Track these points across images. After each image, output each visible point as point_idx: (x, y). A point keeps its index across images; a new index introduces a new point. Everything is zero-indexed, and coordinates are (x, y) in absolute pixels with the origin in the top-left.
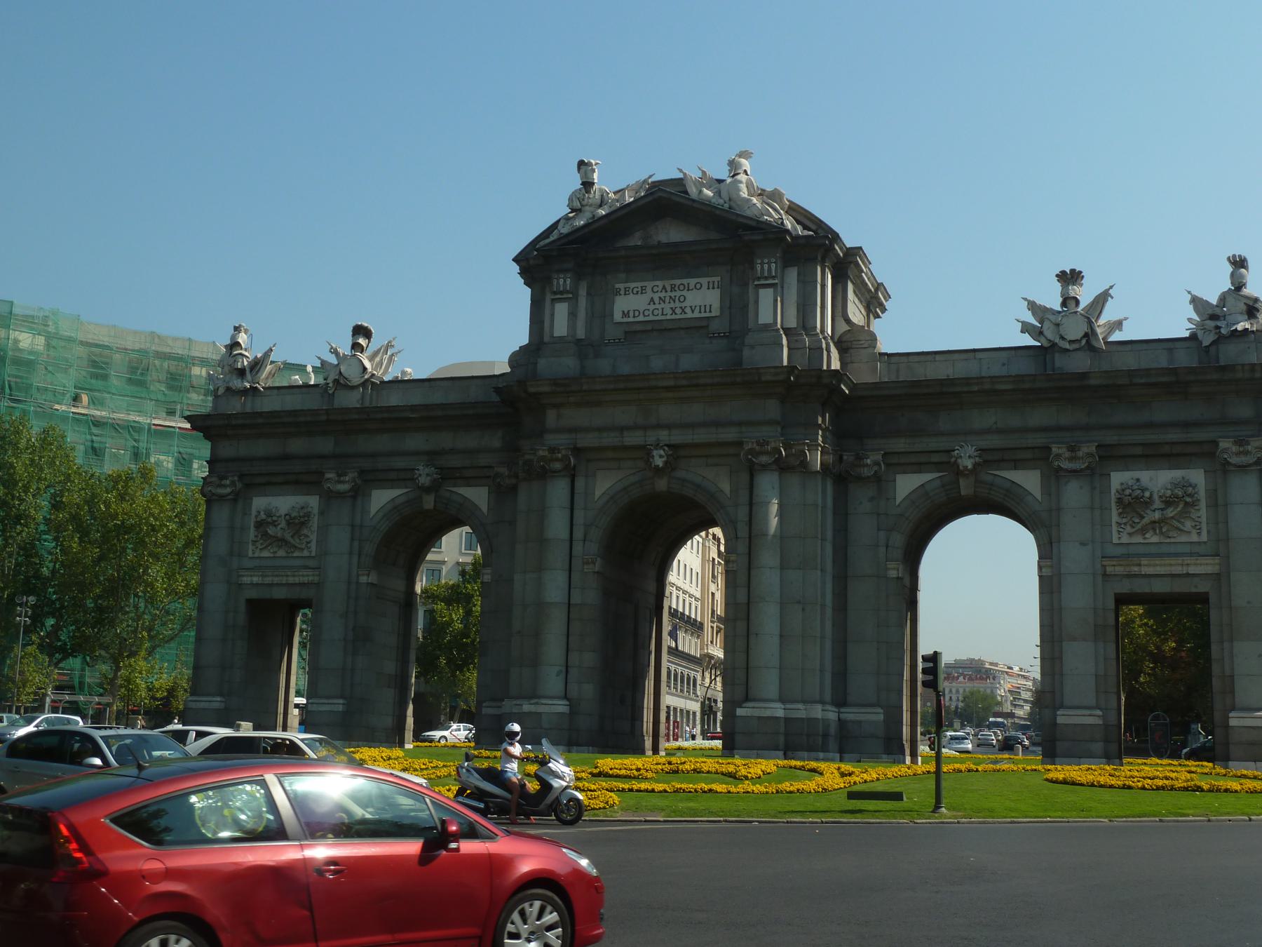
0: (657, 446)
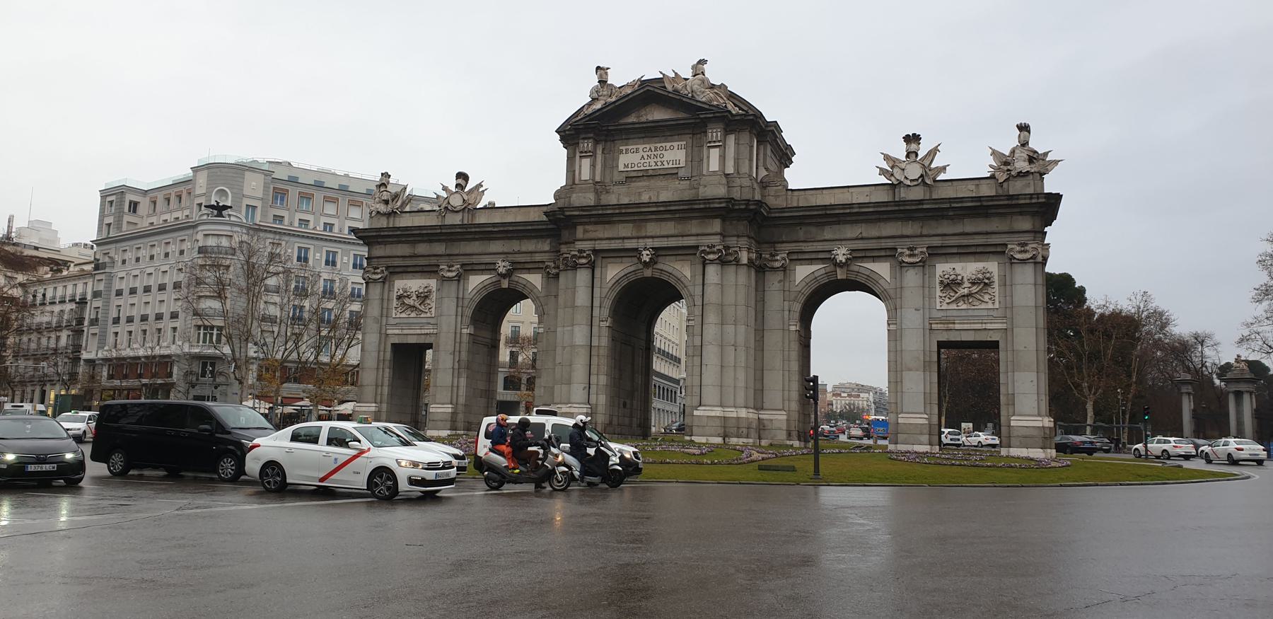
0: (645, 249)
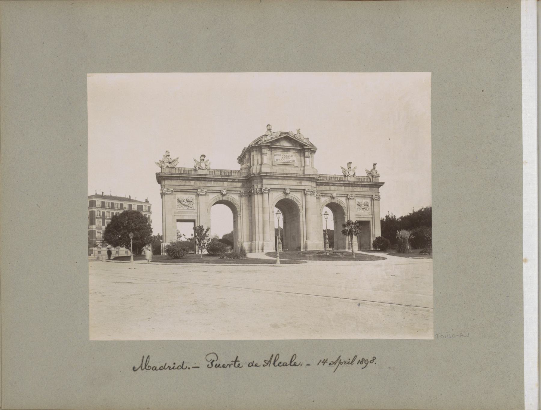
0: (288, 189)
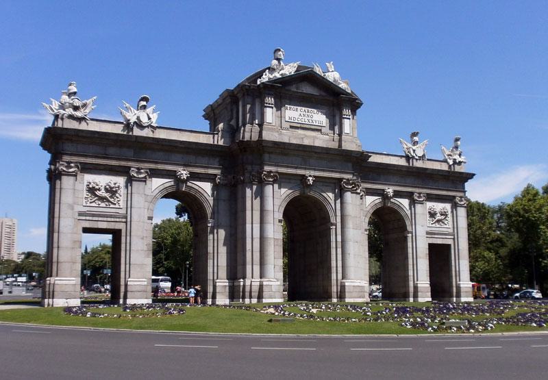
0: (310, 176)
